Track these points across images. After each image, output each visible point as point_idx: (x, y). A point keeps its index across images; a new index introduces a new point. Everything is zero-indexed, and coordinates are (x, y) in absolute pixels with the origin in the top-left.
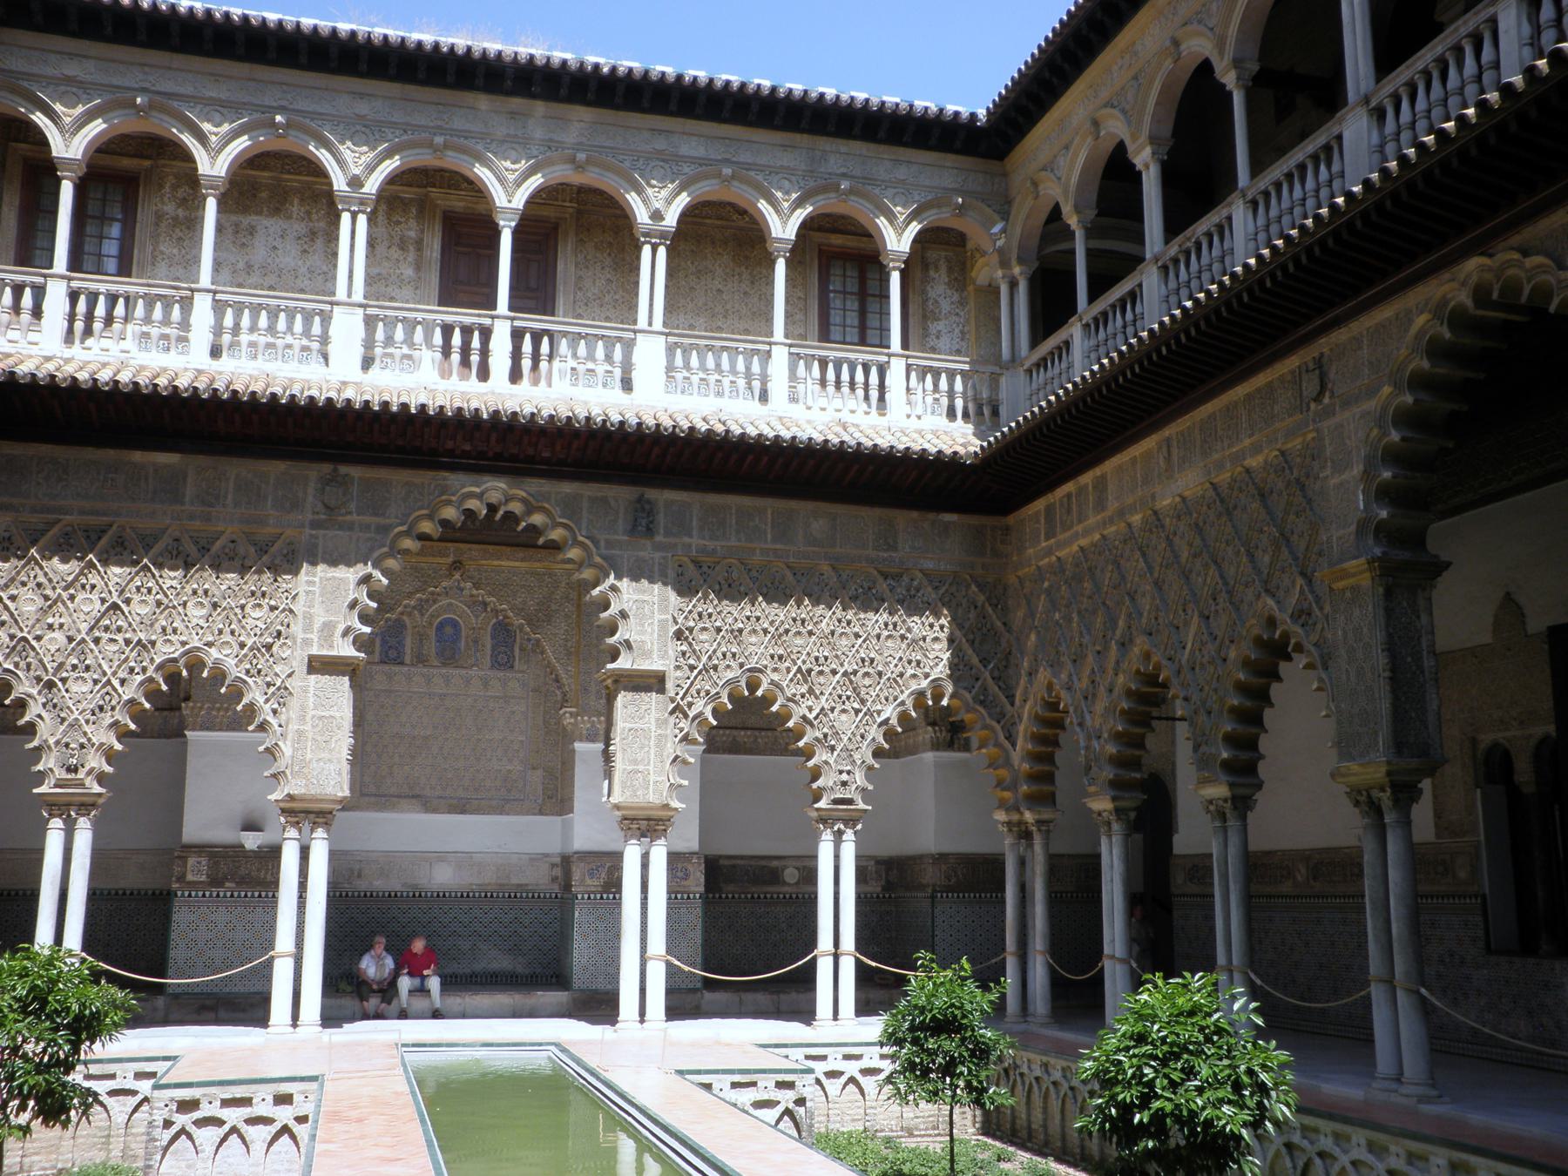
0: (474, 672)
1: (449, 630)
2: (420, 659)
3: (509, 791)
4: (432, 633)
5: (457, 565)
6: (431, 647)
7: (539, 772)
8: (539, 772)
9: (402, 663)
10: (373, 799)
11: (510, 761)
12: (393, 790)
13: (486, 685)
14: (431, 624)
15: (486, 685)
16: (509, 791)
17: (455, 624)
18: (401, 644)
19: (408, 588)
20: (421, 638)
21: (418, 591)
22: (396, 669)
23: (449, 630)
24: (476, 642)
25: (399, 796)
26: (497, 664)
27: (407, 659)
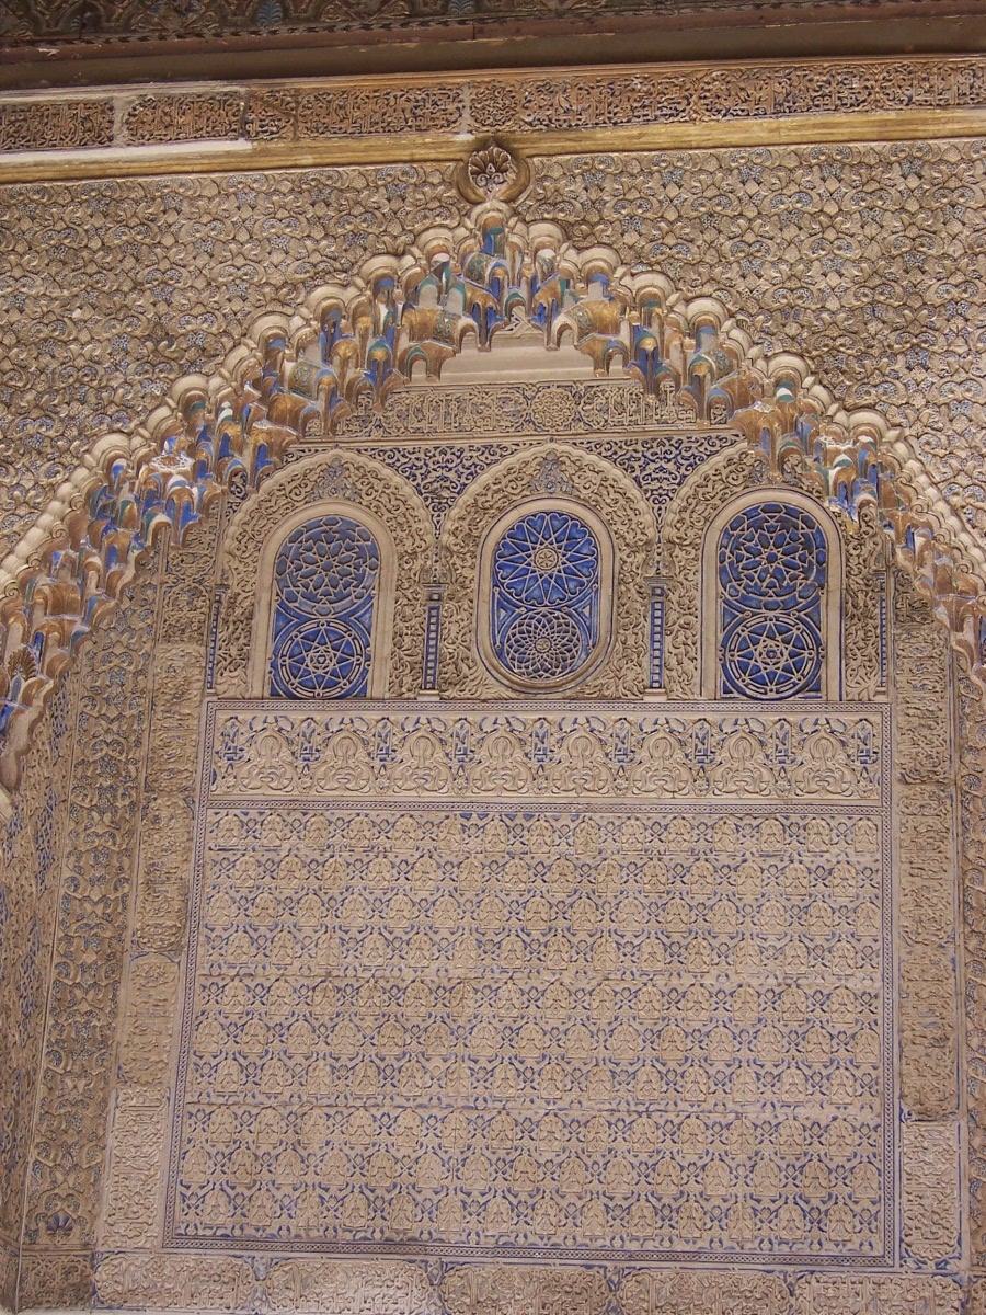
0: (652, 712)
1: (547, 559)
2: (431, 673)
3: (816, 1218)
4: (479, 575)
5: (496, 155)
6: (473, 624)
7: (951, 1135)
8: (951, 1135)
9: (358, 694)
10: (217, 1259)
11: (816, 1081)
12: (307, 1218)
13: (702, 759)
14: (472, 538)
15: (702, 759)
16: (816, 1218)
17: (570, 534)
18: (357, 621)
19: (279, 267)
20: (435, 595)
21: (319, 276)
22: (329, 715)
23: (547, 559)
24: (657, 595)
25: (327, 1246)
26: (744, 677)
27: (378, 683)
